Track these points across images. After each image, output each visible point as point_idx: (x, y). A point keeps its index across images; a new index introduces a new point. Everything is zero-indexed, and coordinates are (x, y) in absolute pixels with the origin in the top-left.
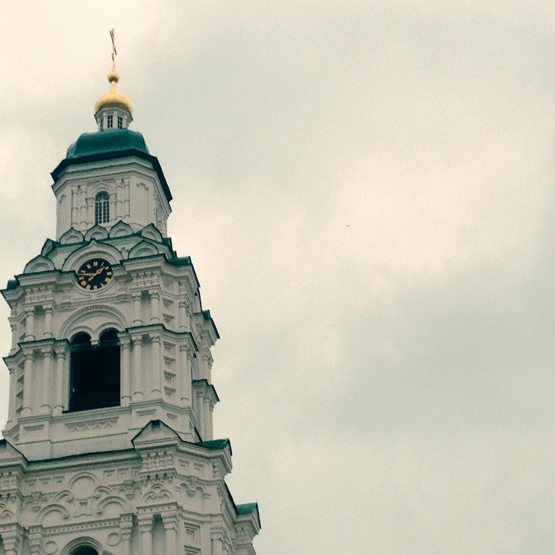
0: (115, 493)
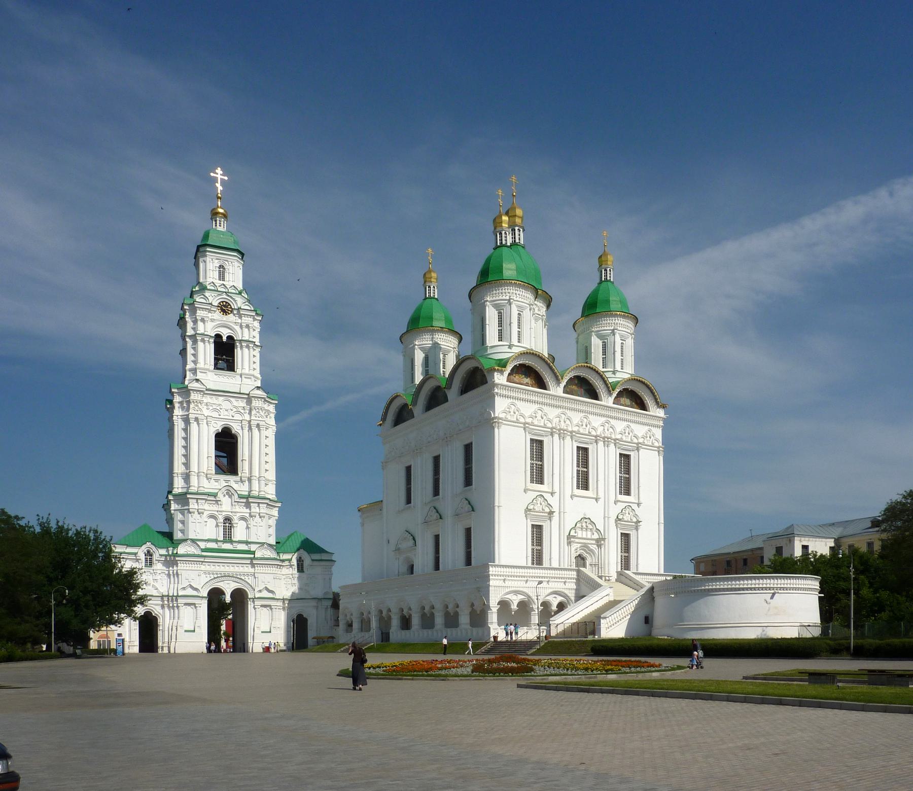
0: (240, 409)
